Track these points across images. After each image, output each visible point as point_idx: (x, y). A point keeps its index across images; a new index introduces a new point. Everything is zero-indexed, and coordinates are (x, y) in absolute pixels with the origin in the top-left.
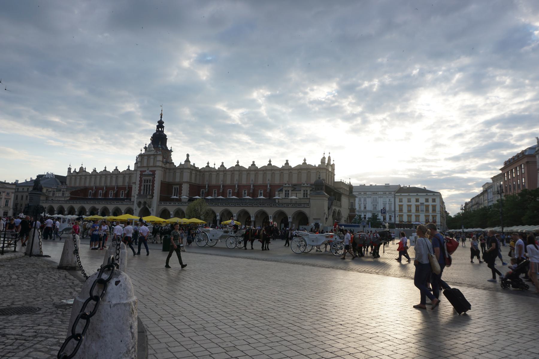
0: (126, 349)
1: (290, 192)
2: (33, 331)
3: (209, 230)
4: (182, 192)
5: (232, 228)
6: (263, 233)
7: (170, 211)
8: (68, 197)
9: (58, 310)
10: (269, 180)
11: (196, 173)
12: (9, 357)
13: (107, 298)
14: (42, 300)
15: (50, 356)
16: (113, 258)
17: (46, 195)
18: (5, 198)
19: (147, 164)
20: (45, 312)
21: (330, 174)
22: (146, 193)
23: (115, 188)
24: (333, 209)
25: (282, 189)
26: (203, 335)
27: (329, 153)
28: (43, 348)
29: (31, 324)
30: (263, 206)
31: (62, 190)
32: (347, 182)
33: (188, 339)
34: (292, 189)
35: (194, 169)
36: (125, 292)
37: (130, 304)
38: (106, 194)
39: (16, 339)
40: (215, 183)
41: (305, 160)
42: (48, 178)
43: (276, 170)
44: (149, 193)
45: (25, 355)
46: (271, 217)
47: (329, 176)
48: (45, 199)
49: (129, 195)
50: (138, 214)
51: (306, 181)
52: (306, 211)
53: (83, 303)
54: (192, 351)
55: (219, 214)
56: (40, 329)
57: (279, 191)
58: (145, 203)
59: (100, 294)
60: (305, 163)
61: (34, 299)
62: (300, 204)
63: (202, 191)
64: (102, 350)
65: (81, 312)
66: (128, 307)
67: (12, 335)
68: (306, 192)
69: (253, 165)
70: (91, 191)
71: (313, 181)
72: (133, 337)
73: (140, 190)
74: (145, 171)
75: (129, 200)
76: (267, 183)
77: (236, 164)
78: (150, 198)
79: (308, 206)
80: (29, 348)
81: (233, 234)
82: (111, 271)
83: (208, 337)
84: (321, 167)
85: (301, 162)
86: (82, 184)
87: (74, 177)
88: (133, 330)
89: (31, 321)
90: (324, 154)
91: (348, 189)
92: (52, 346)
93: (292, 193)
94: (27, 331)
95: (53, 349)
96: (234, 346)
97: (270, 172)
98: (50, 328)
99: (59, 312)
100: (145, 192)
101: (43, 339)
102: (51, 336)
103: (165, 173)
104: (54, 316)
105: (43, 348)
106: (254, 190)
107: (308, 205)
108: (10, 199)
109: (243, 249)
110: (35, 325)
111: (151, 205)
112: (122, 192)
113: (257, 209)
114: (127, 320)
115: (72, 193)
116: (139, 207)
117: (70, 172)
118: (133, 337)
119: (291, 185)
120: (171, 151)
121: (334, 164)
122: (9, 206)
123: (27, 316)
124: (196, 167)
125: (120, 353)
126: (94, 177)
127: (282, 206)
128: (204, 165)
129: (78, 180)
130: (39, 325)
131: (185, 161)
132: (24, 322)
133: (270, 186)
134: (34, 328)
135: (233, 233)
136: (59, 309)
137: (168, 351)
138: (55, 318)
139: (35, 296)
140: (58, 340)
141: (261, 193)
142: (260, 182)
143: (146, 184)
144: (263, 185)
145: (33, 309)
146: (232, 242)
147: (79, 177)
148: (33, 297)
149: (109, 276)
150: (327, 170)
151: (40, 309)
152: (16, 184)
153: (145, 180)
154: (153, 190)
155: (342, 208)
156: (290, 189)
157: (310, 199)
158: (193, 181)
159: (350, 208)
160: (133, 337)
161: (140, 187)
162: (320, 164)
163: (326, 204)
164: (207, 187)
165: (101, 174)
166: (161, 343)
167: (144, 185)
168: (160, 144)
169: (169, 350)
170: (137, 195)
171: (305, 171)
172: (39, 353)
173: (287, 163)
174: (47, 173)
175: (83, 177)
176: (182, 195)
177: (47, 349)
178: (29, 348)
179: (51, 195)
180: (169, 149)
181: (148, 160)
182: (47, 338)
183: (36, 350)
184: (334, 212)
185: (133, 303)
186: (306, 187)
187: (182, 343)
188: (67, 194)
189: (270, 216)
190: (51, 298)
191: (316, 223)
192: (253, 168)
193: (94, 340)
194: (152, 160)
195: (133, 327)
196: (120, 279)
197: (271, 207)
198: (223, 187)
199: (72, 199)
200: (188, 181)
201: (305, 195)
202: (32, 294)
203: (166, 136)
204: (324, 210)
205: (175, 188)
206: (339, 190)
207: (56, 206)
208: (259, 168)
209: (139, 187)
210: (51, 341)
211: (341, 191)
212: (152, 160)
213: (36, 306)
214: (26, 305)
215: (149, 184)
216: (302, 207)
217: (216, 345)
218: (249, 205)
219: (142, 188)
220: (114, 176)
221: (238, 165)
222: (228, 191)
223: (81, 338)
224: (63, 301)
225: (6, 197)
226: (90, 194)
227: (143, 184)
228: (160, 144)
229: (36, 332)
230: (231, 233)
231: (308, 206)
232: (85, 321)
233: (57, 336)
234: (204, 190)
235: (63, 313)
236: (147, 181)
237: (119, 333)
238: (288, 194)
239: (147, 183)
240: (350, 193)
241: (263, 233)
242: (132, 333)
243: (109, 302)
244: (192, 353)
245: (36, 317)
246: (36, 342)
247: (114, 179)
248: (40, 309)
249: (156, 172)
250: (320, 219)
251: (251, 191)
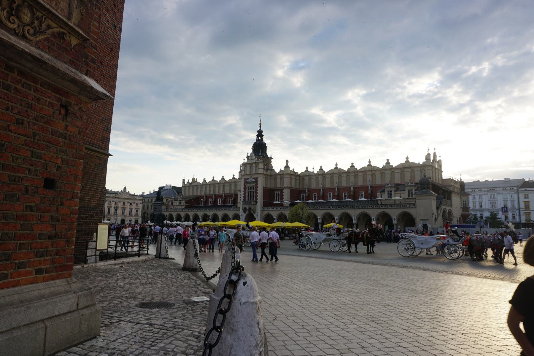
0: (255, 342)
1: (393, 193)
2: (172, 323)
3: (312, 234)
4: (283, 197)
5: (335, 231)
6: (367, 236)
7: (273, 216)
8: (184, 205)
9: (187, 306)
10: (369, 181)
11: (296, 178)
12: (158, 343)
13: (238, 296)
14: (174, 296)
15: (188, 345)
16: (239, 262)
17: (166, 205)
18: (136, 208)
19: (250, 172)
20: (178, 307)
21: (437, 171)
22: (252, 200)
23: (222, 195)
24: (443, 209)
25: (385, 189)
26: (316, 336)
27: (435, 149)
28: (181, 338)
29: (169, 317)
30: (365, 208)
31: (179, 199)
32: (457, 178)
33: (303, 339)
34: (396, 189)
35: (293, 174)
36: (252, 292)
37: (256, 303)
38: (215, 202)
39: (161, 329)
40: (314, 187)
41: (407, 158)
42: (167, 189)
43: (377, 170)
44: (253, 199)
45: (169, 342)
46: (373, 219)
47: (435, 173)
48: (166, 208)
49: (235, 202)
50: (244, 219)
51: (410, 181)
52: (412, 211)
53: (218, 300)
54: (308, 350)
55: (320, 217)
56: (176, 322)
57: (381, 192)
58: (250, 209)
59: (232, 293)
60: (407, 161)
61: (168, 295)
62: (405, 205)
63: (303, 195)
64: (235, 342)
65: (218, 308)
66: (255, 305)
67: (157, 325)
68: (410, 192)
69: (352, 166)
70: (202, 199)
71: (418, 179)
72: (260, 333)
73: (245, 197)
74: (249, 179)
75: (235, 207)
76: (368, 184)
77: (335, 166)
78: (254, 204)
79: (414, 207)
80: (171, 337)
81: (336, 237)
82: (239, 273)
83: (322, 338)
84: (426, 165)
85: (403, 161)
86: (195, 194)
87: (187, 188)
88: (260, 326)
89: (169, 314)
90: (429, 150)
91: (459, 186)
92: (188, 337)
93: (395, 193)
94: (167, 322)
95: (189, 339)
96: (348, 349)
97: (370, 173)
98: (184, 321)
99: (189, 308)
100: (249, 199)
101: (180, 330)
102: (186, 328)
103: (267, 179)
104: (186, 311)
105: (181, 338)
106: (354, 192)
107: (414, 205)
108: (139, 209)
109: (348, 253)
110: (173, 318)
111: (255, 210)
112: (229, 199)
113: (358, 212)
114: (255, 317)
115: (186, 202)
116: (245, 212)
117: (185, 183)
118: (260, 332)
119: (393, 185)
120: (271, 158)
121: (440, 161)
122: (138, 215)
123: (165, 310)
124: (295, 172)
125: (251, 346)
126: (204, 186)
127: (385, 207)
128: (303, 170)
129: (191, 190)
130: (175, 318)
131: (285, 167)
132: (164, 315)
133: (371, 187)
134: (172, 320)
135: (336, 236)
136: (189, 306)
137: (285, 348)
138: (186, 313)
139: (167, 293)
140: (191, 332)
141: (362, 195)
142: (360, 183)
143: (250, 191)
144: (364, 187)
145: (168, 304)
146: (335, 245)
147: (191, 187)
148: (167, 294)
149: (237, 277)
150: (433, 167)
151: (174, 305)
152: (142, 196)
153: (249, 187)
154: (256, 196)
155: (453, 208)
156: (393, 190)
157: (415, 198)
158: (293, 186)
159: (463, 206)
160: (260, 332)
161: (245, 194)
162: (425, 161)
163: (434, 203)
164: (307, 191)
165: (210, 183)
166: (278, 340)
167: (249, 192)
168: (260, 152)
169: (286, 348)
170: (242, 201)
171: (409, 170)
172: (179, 342)
173: (388, 163)
174: (166, 185)
175: (195, 187)
176: (284, 200)
177: (185, 339)
178: (171, 337)
179: (170, 204)
180: (269, 156)
181: (250, 168)
182: (183, 330)
183: (177, 339)
184: (444, 212)
185: (258, 303)
186: (411, 186)
187: (298, 342)
188: (183, 203)
189: (373, 218)
190: (181, 296)
191: (423, 224)
192: (352, 170)
193: (229, 333)
194: (254, 168)
195: (260, 324)
196: (246, 280)
197: (373, 208)
199: (187, 207)
200: (289, 186)
201: (410, 194)
202: (166, 291)
203: (265, 144)
204: (433, 210)
205: (277, 193)
206: (448, 188)
207: (174, 214)
208: (358, 169)
209: (244, 194)
210: (187, 333)
211: (451, 189)
212: (254, 168)
213: (171, 302)
214: (162, 300)
215: (252, 191)
216: (407, 208)
217: (330, 346)
218: (350, 207)
219: (247, 194)
220: (222, 185)
221: (336, 168)
222: (328, 195)
223: (221, 330)
224: (190, 298)
225: (136, 207)
226: (202, 202)
227: (247, 191)
228: (260, 152)
229: (174, 324)
230: (334, 236)
231: (414, 207)
232: (222, 315)
233: (190, 328)
234: (304, 194)
235: (192, 309)
236: (251, 187)
237: (249, 328)
238: (391, 194)
239: (251, 189)
240: (461, 191)
241: (367, 236)
242: (260, 329)
243: (239, 300)
244: (308, 352)
245: (172, 311)
246: (175, 333)
247: (221, 188)
248: (174, 305)
249: (258, 179)
250: (428, 220)
251: (352, 193)
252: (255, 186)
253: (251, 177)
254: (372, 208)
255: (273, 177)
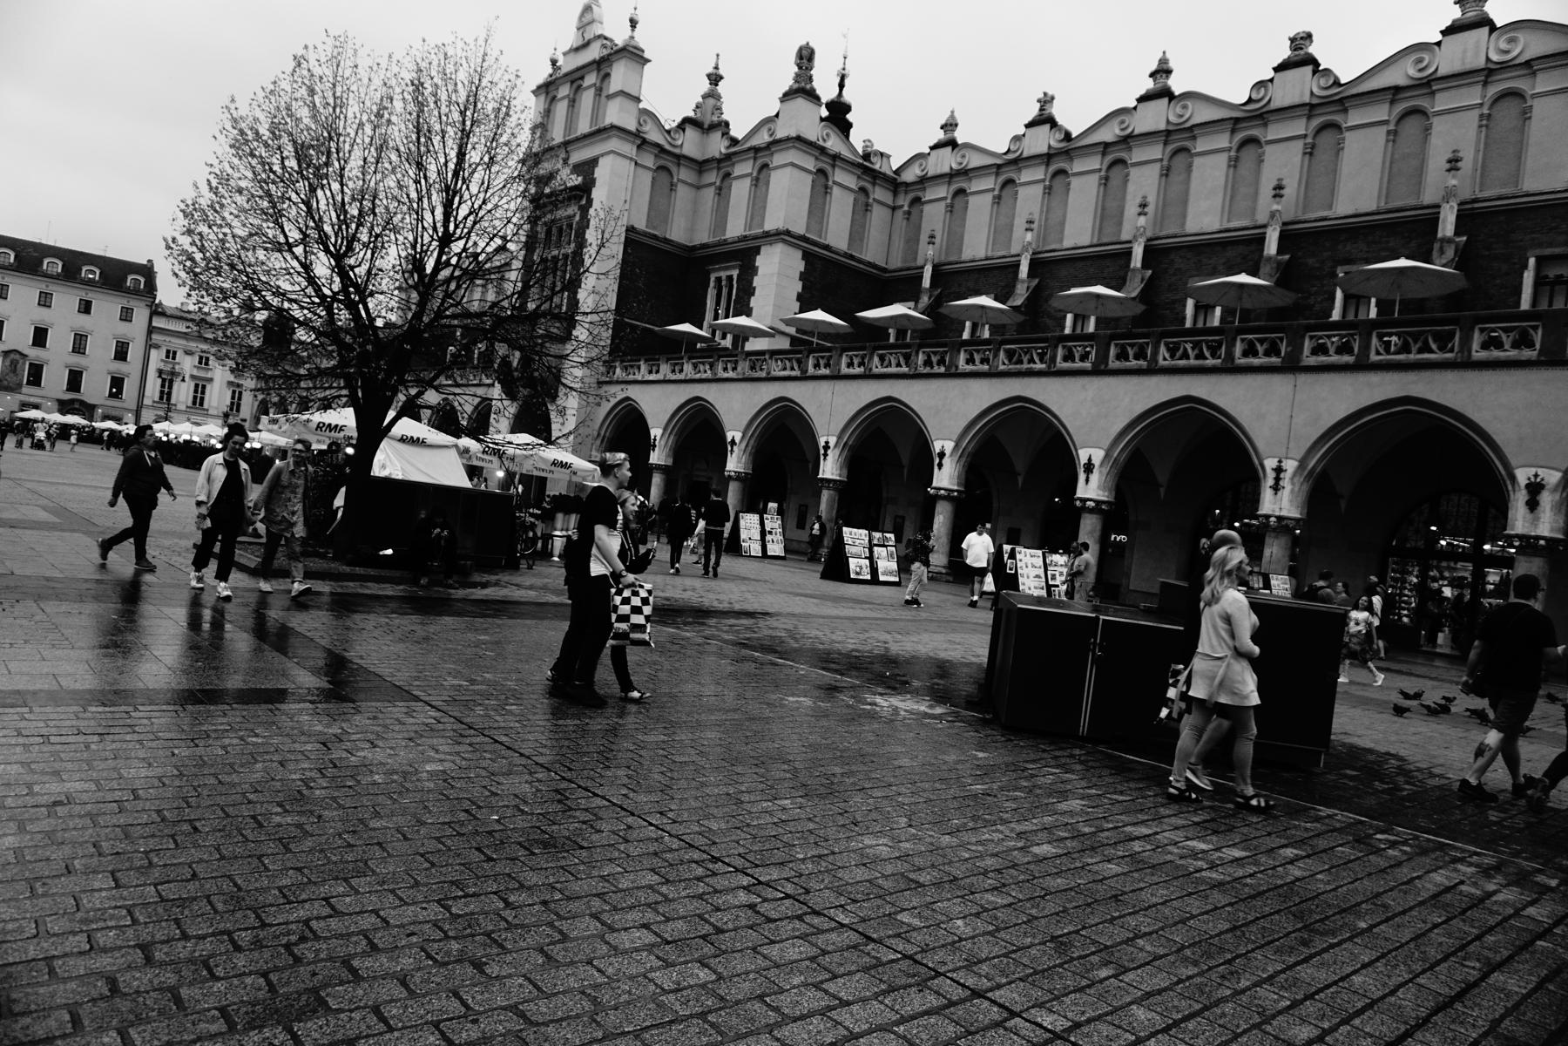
46: (1535, 488)
164: (926, 283)
189: (1523, 476)
198: (1031, 274)
200: (799, 228)
252: (577, 218)
253: (565, 161)
254: (1527, 354)
255: (712, 177)
